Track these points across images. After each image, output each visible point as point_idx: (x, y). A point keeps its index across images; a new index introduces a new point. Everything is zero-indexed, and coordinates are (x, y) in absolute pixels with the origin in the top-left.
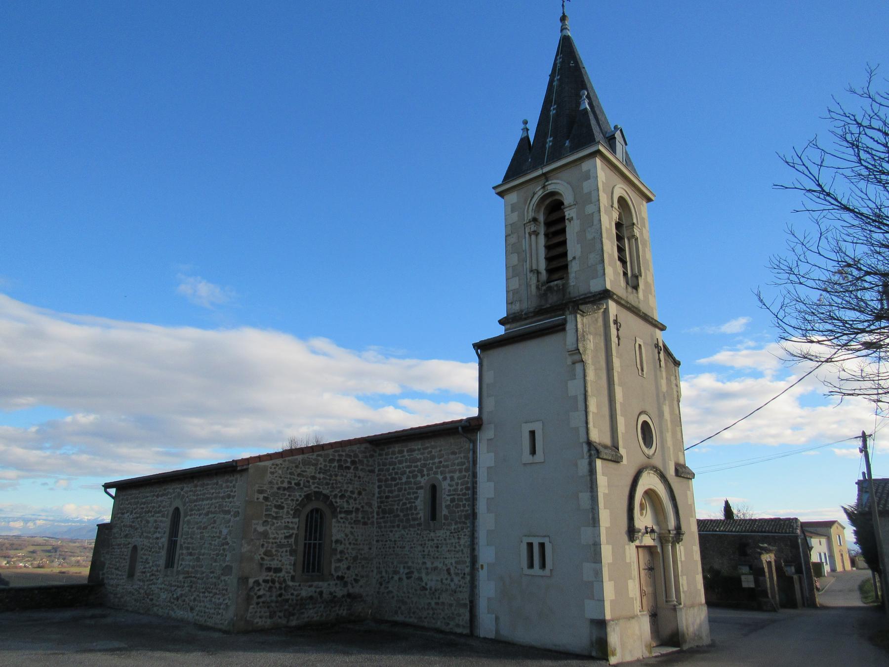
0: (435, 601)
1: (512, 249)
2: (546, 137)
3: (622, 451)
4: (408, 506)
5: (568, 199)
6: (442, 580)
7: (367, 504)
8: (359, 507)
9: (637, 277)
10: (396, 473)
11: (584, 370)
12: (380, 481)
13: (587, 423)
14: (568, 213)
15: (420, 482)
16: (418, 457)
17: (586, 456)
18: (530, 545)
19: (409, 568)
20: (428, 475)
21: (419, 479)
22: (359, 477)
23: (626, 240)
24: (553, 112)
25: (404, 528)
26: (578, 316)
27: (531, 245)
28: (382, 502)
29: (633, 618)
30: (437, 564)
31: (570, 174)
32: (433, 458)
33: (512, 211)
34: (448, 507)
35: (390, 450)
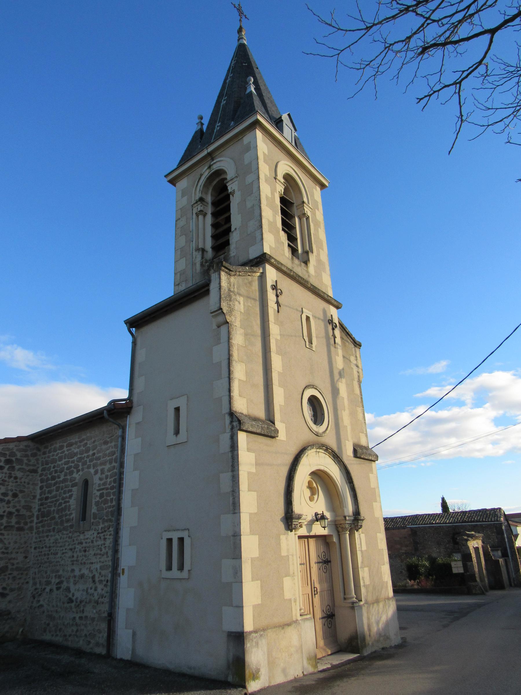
0: (79, 615)
1: (182, 231)
2: (216, 122)
3: (279, 425)
4: (63, 505)
5: (230, 174)
6: (87, 589)
7: (24, 507)
8: (13, 510)
9: (307, 253)
10: (56, 472)
11: (229, 333)
12: (42, 481)
13: (230, 391)
14: (231, 187)
15: (75, 478)
16: (75, 451)
17: (228, 430)
18: (170, 541)
19: (60, 577)
20: (83, 469)
21: (75, 475)
22: (16, 478)
23: (297, 219)
24: (223, 102)
25: (59, 531)
26: (223, 274)
27: (197, 226)
28: (42, 505)
29: (289, 625)
30: (85, 572)
31: (234, 150)
32: (87, 451)
33: (183, 196)
34: (97, 503)
35: (53, 447)
